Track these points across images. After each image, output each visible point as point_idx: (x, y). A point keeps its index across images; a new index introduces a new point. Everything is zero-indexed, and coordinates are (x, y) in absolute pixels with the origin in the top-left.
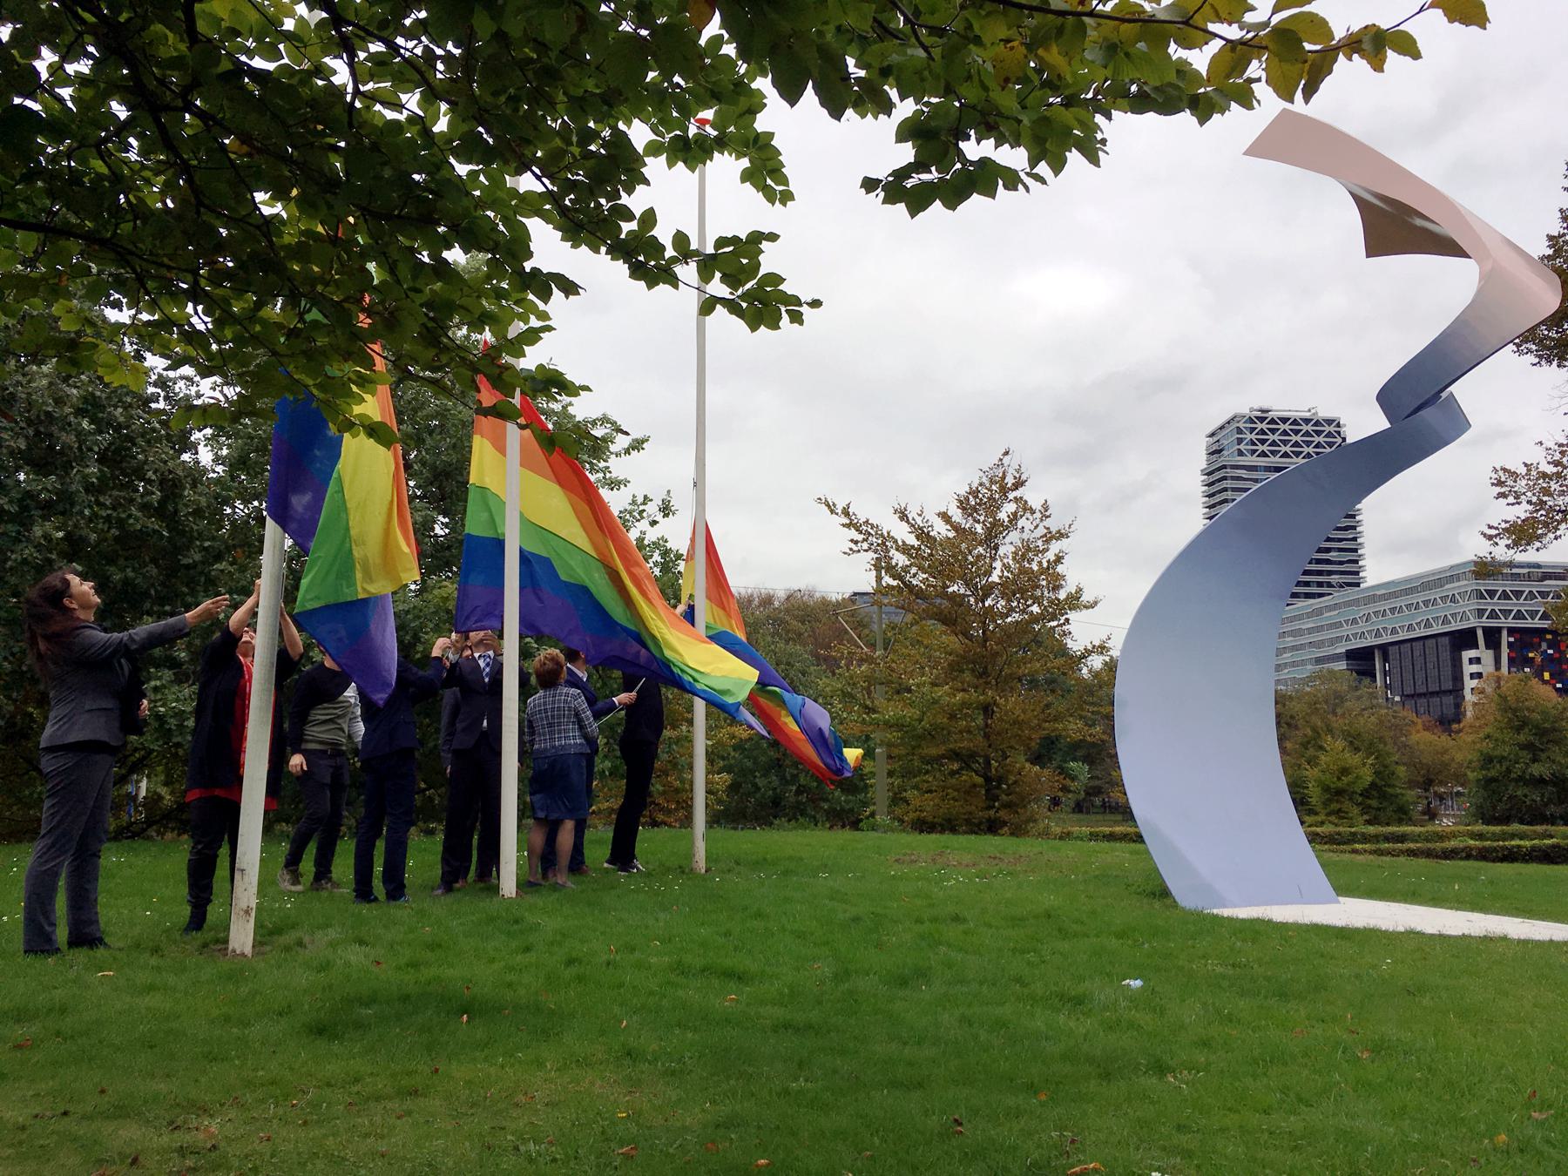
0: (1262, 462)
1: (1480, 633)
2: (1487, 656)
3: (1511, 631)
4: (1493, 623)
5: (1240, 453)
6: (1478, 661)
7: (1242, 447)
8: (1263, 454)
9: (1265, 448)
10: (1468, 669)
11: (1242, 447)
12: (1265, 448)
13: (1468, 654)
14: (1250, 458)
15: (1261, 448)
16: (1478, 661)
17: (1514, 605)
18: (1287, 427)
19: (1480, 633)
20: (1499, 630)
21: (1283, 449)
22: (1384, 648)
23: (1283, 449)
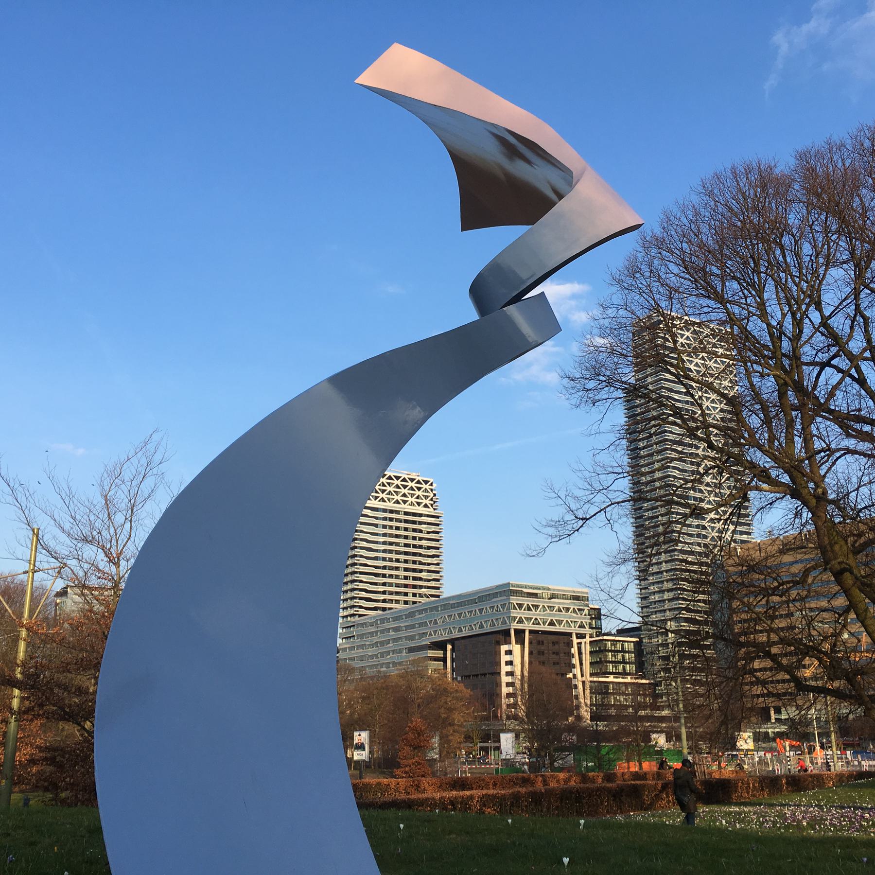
0: (381, 505)
1: (512, 632)
2: (516, 648)
3: (531, 632)
4: (520, 626)
6: (509, 652)
8: (383, 500)
10: (504, 658)
12: (384, 496)
13: (504, 648)
16: (509, 652)
17: (533, 614)
18: (399, 482)
19: (512, 632)
20: (523, 631)
21: (396, 497)
22: (452, 641)
23: (396, 497)
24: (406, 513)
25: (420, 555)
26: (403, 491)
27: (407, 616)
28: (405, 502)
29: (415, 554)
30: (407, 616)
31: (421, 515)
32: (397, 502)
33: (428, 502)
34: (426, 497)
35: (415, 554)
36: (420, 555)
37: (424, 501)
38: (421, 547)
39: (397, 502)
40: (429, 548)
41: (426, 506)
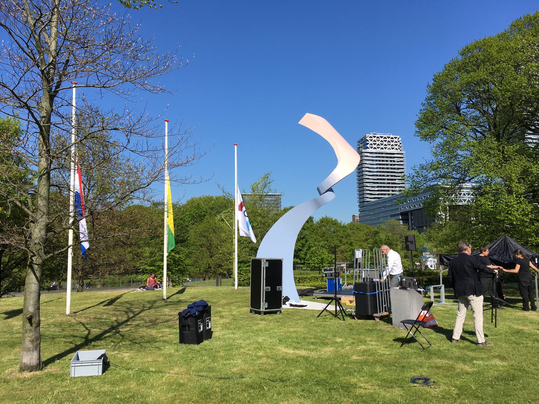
0: (374, 151)
5: (368, 148)
7: (368, 146)
8: (375, 148)
9: (376, 146)
11: (368, 146)
12: (376, 146)
14: (371, 149)
15: (374, 146)
21: (381, 146)
23: (381, 146)
24: (387, 154)
25: (395, 172)
26: (385, 143)
27: (389, 201)
28: (385, 148)
29: (392, 172)
30: (389, 201)
31: (394, 154)
32: (382, 148)
33: (397, 147)
34: (396, 145)
35: (392, 172)
36: (395, 172)
37: (395, 147)
38: (394, 169)
39: (382, 148)
40: (398, 169)
41: (397, 149)
